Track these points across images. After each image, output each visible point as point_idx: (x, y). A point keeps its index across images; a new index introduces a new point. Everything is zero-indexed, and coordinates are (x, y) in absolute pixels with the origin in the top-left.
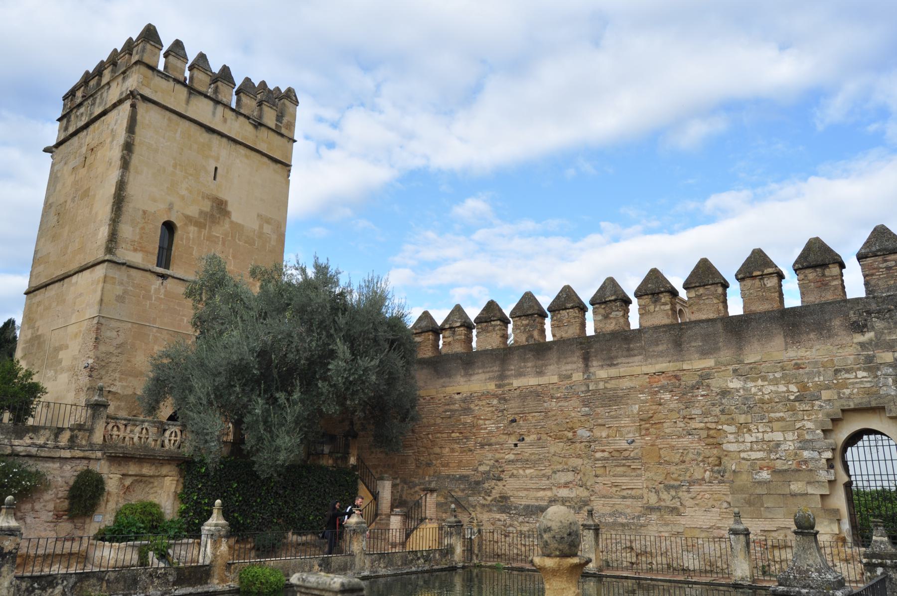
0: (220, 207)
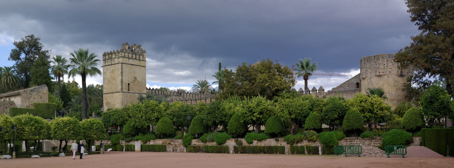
0: (135, 78)
